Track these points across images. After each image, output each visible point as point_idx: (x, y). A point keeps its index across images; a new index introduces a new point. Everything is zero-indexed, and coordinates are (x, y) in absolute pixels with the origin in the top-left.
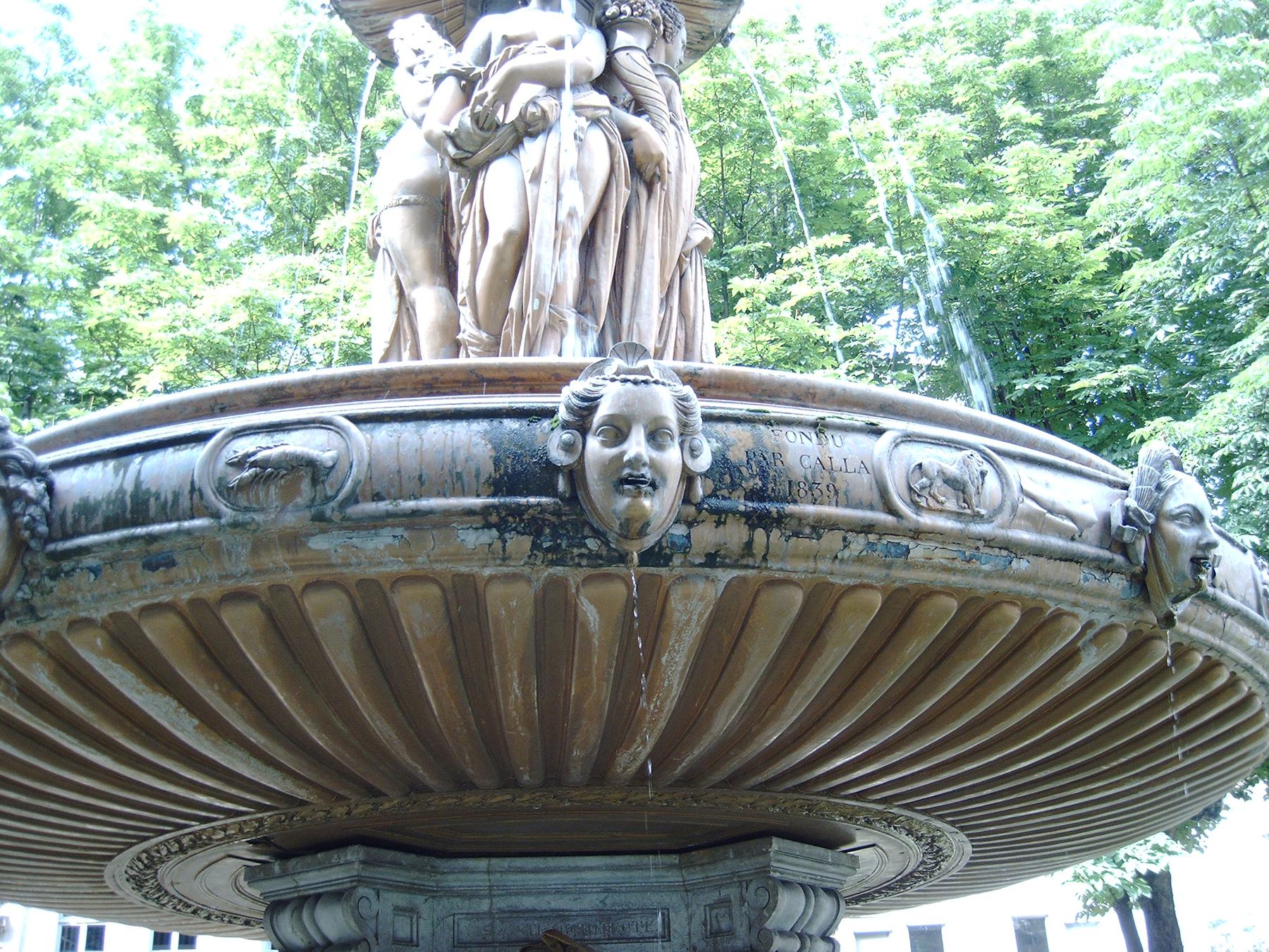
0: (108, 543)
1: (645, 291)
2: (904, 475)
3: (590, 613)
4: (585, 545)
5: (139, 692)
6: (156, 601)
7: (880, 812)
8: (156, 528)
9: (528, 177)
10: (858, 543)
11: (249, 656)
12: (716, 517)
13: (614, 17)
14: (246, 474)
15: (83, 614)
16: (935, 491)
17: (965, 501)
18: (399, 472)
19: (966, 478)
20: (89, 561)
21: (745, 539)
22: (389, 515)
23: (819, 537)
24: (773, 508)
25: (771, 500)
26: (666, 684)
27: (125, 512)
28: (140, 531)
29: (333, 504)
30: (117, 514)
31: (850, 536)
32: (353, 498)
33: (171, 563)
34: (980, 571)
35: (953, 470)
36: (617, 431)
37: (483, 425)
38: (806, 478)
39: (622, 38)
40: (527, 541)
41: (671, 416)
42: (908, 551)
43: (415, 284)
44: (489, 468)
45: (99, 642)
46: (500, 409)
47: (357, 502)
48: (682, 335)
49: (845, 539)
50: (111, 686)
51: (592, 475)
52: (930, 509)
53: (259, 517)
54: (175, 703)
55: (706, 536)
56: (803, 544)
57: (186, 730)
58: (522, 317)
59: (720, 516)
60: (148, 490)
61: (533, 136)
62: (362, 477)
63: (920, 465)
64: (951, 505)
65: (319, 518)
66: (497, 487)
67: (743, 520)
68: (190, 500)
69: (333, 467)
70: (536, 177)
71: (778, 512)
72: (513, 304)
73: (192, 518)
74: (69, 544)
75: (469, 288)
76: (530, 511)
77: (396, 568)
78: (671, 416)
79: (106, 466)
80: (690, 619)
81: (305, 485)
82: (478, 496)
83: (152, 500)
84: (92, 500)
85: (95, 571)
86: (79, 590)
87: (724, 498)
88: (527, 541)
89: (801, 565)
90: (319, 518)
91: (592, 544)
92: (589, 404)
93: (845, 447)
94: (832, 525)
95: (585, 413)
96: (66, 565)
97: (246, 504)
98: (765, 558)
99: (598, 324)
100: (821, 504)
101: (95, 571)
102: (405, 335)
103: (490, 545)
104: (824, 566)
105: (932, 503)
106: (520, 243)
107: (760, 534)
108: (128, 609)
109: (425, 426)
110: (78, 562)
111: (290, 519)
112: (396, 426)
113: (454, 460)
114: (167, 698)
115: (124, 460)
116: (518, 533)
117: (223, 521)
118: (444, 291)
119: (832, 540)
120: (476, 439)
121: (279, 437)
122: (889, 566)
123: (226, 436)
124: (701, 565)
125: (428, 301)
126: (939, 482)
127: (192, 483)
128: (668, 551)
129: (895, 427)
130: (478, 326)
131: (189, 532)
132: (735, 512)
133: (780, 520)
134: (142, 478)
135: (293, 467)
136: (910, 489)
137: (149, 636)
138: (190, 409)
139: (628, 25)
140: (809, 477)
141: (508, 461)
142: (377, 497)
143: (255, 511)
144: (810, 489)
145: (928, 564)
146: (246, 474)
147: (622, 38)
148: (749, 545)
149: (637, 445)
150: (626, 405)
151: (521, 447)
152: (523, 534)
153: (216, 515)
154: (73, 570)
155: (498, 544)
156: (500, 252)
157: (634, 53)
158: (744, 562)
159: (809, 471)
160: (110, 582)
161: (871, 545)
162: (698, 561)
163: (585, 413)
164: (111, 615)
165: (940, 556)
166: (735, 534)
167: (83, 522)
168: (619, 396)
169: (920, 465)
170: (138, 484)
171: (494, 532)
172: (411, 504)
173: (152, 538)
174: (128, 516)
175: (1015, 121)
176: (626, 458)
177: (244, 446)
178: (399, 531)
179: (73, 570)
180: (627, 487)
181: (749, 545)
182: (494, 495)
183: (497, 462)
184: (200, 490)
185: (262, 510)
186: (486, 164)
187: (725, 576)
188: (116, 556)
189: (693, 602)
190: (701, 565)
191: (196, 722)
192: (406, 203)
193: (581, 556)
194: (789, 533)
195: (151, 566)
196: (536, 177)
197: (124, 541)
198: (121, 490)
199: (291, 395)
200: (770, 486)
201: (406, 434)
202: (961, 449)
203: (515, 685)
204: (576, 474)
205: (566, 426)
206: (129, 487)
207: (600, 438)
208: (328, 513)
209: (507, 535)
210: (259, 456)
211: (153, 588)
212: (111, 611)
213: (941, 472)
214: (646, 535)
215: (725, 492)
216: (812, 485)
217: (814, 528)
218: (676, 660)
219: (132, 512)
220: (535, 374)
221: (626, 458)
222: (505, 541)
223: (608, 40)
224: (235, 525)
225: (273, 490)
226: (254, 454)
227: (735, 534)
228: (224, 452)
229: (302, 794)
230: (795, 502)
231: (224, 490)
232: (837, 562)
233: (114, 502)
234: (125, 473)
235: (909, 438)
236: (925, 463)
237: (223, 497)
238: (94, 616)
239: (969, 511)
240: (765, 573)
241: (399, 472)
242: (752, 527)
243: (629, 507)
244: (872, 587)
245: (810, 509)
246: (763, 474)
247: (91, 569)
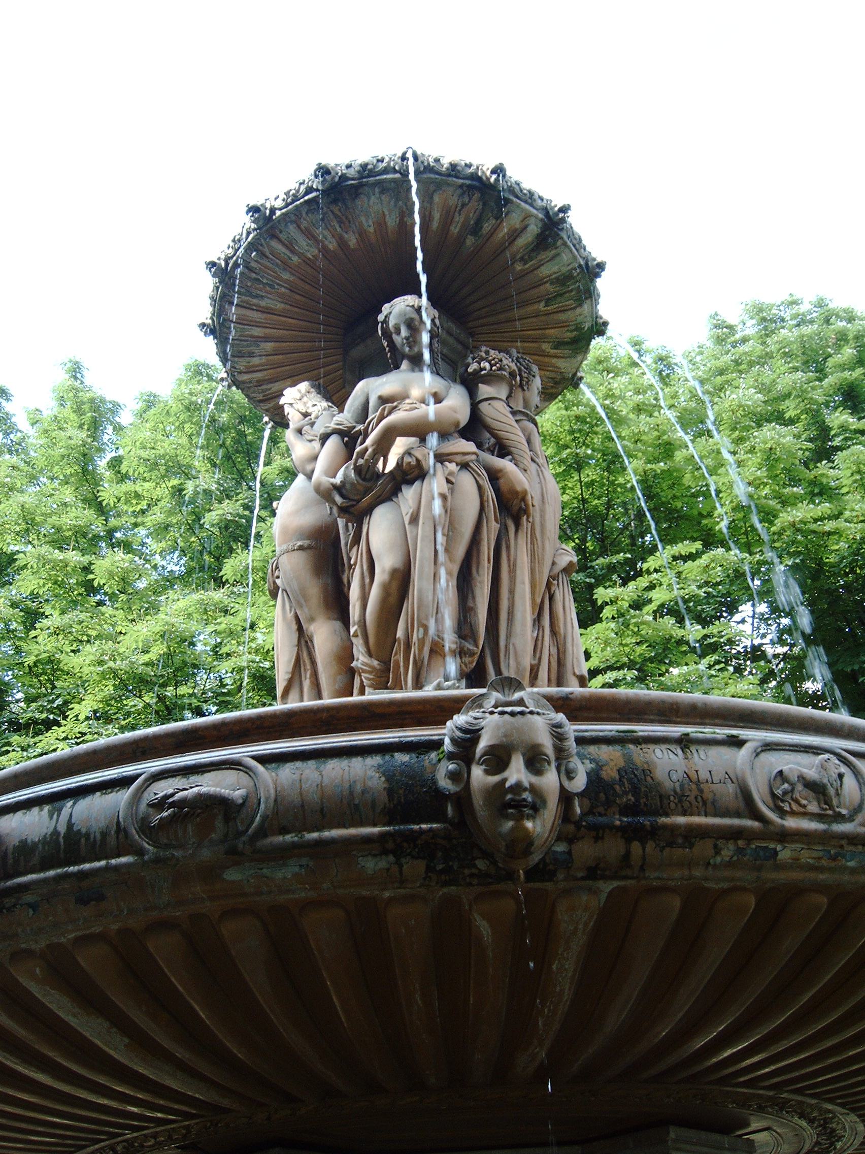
0: (45, 881)
1: (518, 615)
2: (766, 782)
3: (484, 927)
4: (475, 866)
5: (74, 1015)
7: (770, 1098)
8: (87, 866)
9: (407, 520)
10: (728, 851)
11: (173, 980)
12: (593, 833)
13: (476, 372)
14: (165, 814)
15: (23, 946)
16: (797, 795)
17: (826, 804)
18: (302, 806)
19: (825, 781)
20: (29, 898)
21: (622, 851)
22: (294, 846)
23: (691, 846)
24: (646, 821)
25: (644, 814)
26: (558, 989)
29: (244, 838)
31: (720, 843)
32: (263, 832)
33: (101, 898)
34: (846, 868)
35: (812, 774)
36: (498, 759)
37: (375, 760)
38: (675, 791)
39: (485, 390)
40: (421, 865)
41: (547, 743)
42: (776, 853)
43: (312, 620)
44: (384, 797)
45: (38, 970)
46: (391, 744)
47: (266, 836)
48: (554, 651)
49: (715, 846)
50: (50, 1010)
51: (478, 801)
52: (793, 813)
53: (178, 853)
54: (106, 1024)
55: (586, 850)
56: (678, 853)
57: (117, 1049)
58: (408, 646)
59: (598, 832)
61: (411, 483)
62: (268, 813)
63: (781, 772)
64: (813, 808)
65: (233, 851)
66: (391, 815)
67: (620, 834)
68: (114, 839)
69: (243, 804)
70: (414, 519)
71: (652, 825)
72: (400, 634)
73: (119, 856)
75: (360, 621)
76: (423, 837)
77: (303, 894)
78: (547, 743)
79: (42, 810)
80: (576, 928)
81: (219, 823)
82: (375, 825)
83: (83, 840)
85: (34, 906)
87: (600, 815)
88: (421, 865)
89: (677, 874)
90: (233, 851)
91: (481, 864)
92: (471, 735)
93: (710, 760)
94: (702, 833)
95: (468, 744)
97: (165, 841)
98: (642, 868)
99: (477, 646)
100: (691, 815)
102: (305, 666)
103: (388, 870)
104: (698, 873)
105: (795, 807)
106: (402, 578)
107: (636, 847)
108: (63, 940)
109: (324, 763)
111: (206, 854)
112: (298, 764)
113: (351, 793)
114: (99, 1020)
115: (57, 804)
116: (413, 857)
117: (146, 857)
118: (338, 624)
119: (704, 848)
120: (371, 773)
121: (193, 779)
122: (759, 869)
123: (146, 780)
124: (583, 878)
125: (323, 635)
126: (800, 787)
127: (118, 822)
128: (551, 867)
129: (755, 736)
130: (370, 654)
131: (116, 868)
132: (612, 827)
133: (655, 832)
134: (73, 821)
135: (207, 806)
136: (773, 795)
137: (83, 964)
139: (490, 379)
140: (678, 790)
141: (401, 792)
142: (284, 831)
143: (175, 847)
144: (680, 801)
145: (796, 864)
146: (165, 814)
147: (485, 390)
148: (627, 856)
149: (517, 772)
150: (506, 736)
151: (412, 777)
152: (417, 858)
153: (140, 852)
154: (14, 906)
155: (395, 868)
156: (386, 588)
157: (496, 404)
158: (624, 873)
159: (677, 785)
161: (740, 851)
162: (580, 874)
163: (468, 744)
164: (48, 946)
165: (807, 856)
166: (613, 848)
168: (498, 727)
169: (781, 772)
170: (70, 825)
171: (391, 858)
172: (315, 835)
173: (82, 874)
174: (62, 856)
175: (844, 428)
176: (507, 785)
177: (163, 788)
178: (304, 861)
179: (14, 906)
180: (510, 811)
181: (627, 856)
182: (389, 824)
183: (390, 792)
184: (125, 830)
185: (181, 846)
186: (369, 511)
187: (606, 887)
189: (578, 914)
190: (583, 878)
191: (127, 1040)
192: (301, 548)
193: (472, 875)
194: (663, 844)
195: (83, 901)
196: (414, 519)
198: (55, 832)
200: (643, 801)
201: (307, 772)
202: (819, 754)
203: (418, 997)
204: (463, 799)
205: (451, 757)
206: (62, 829)
207: (483, 767)
208: (240, 846)
209: (403, 860)
210: (177, 797)
212: (48, 942)
213: (801, 778)
214: (531, 853)
215: (601, 809)
216: (681, 797)
217: (686, 837)
218: (566, 968)
220: (420, 707)
221: (507, 785)
222: (401, 866)
223: (472, 392)
224: (157, 861)
225: (190, 828)
226: (172, 795)
227: (613, 848)
228: (146, 795)
229: (225, 1103)
230: (667, 815)
231: (145, 827)
232: (710, 868)
234: (58, 816)
235: (769, 747)
236: (785, 768)
237: (146, 837)
238: (33, 947)
239: (830, 812)
240: (643, 882)
241: (302, 806)
242: (628, 841)
243: (513, 829)
244: (744, 889)
245: (681, 820)
246: (635, 790)
247: (30, 905)
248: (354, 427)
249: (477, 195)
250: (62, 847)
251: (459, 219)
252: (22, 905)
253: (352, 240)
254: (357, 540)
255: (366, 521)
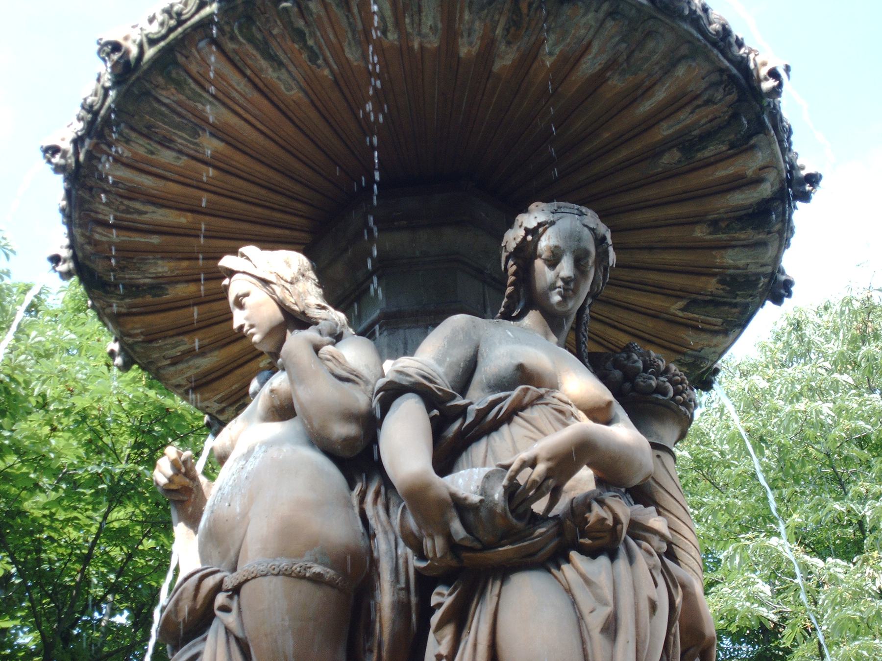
9: (595, 621)
70: (611, 628)
186: (504, 571)
192: (317, 579)
196: (611, 628)
248: (453, 397)
249: (734, 96)
251: (685, 118)
253: (506, 58)
254: (459, 617)
255: (493, 589)
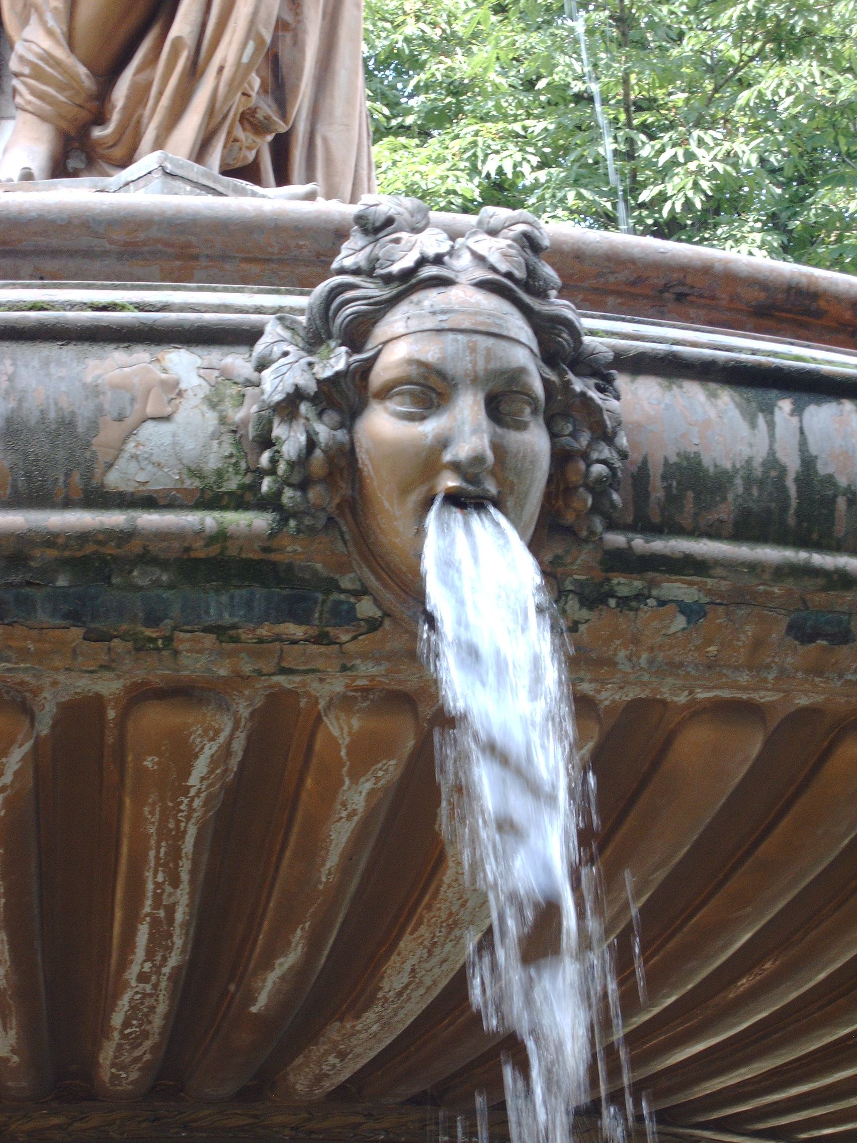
0: (754, 567)
6: (745, 696)
20: (677, 589)
27: (784, 508)
28: (819, 559)
30: (769, 511)
60: (830, 480)
74: (660, 545)
84: (707, 462)
85: (692, 612)
86: (636, 641)
96: (625, 584)
101: (692, 612)
110: (652, 584)
134: (813, 449)
138: (623, 276)
154: (641, 597)
160: (710, 642)
167: (689, 506)
174: (791, 521)
179: (641, 597)
188: (743, 590)
195: (802, 632)
197: (782, 571)
198: (772, 462)
199: (818, 314)
211: (782, 670)
219: (799, 514)
233: (761, 483)
234: (771, 425)
250: (794, 502)
252: (662, 603)
